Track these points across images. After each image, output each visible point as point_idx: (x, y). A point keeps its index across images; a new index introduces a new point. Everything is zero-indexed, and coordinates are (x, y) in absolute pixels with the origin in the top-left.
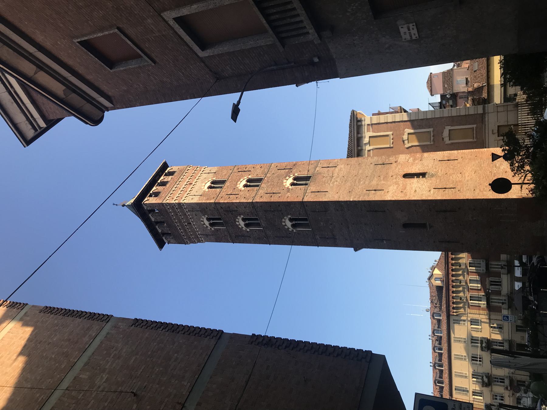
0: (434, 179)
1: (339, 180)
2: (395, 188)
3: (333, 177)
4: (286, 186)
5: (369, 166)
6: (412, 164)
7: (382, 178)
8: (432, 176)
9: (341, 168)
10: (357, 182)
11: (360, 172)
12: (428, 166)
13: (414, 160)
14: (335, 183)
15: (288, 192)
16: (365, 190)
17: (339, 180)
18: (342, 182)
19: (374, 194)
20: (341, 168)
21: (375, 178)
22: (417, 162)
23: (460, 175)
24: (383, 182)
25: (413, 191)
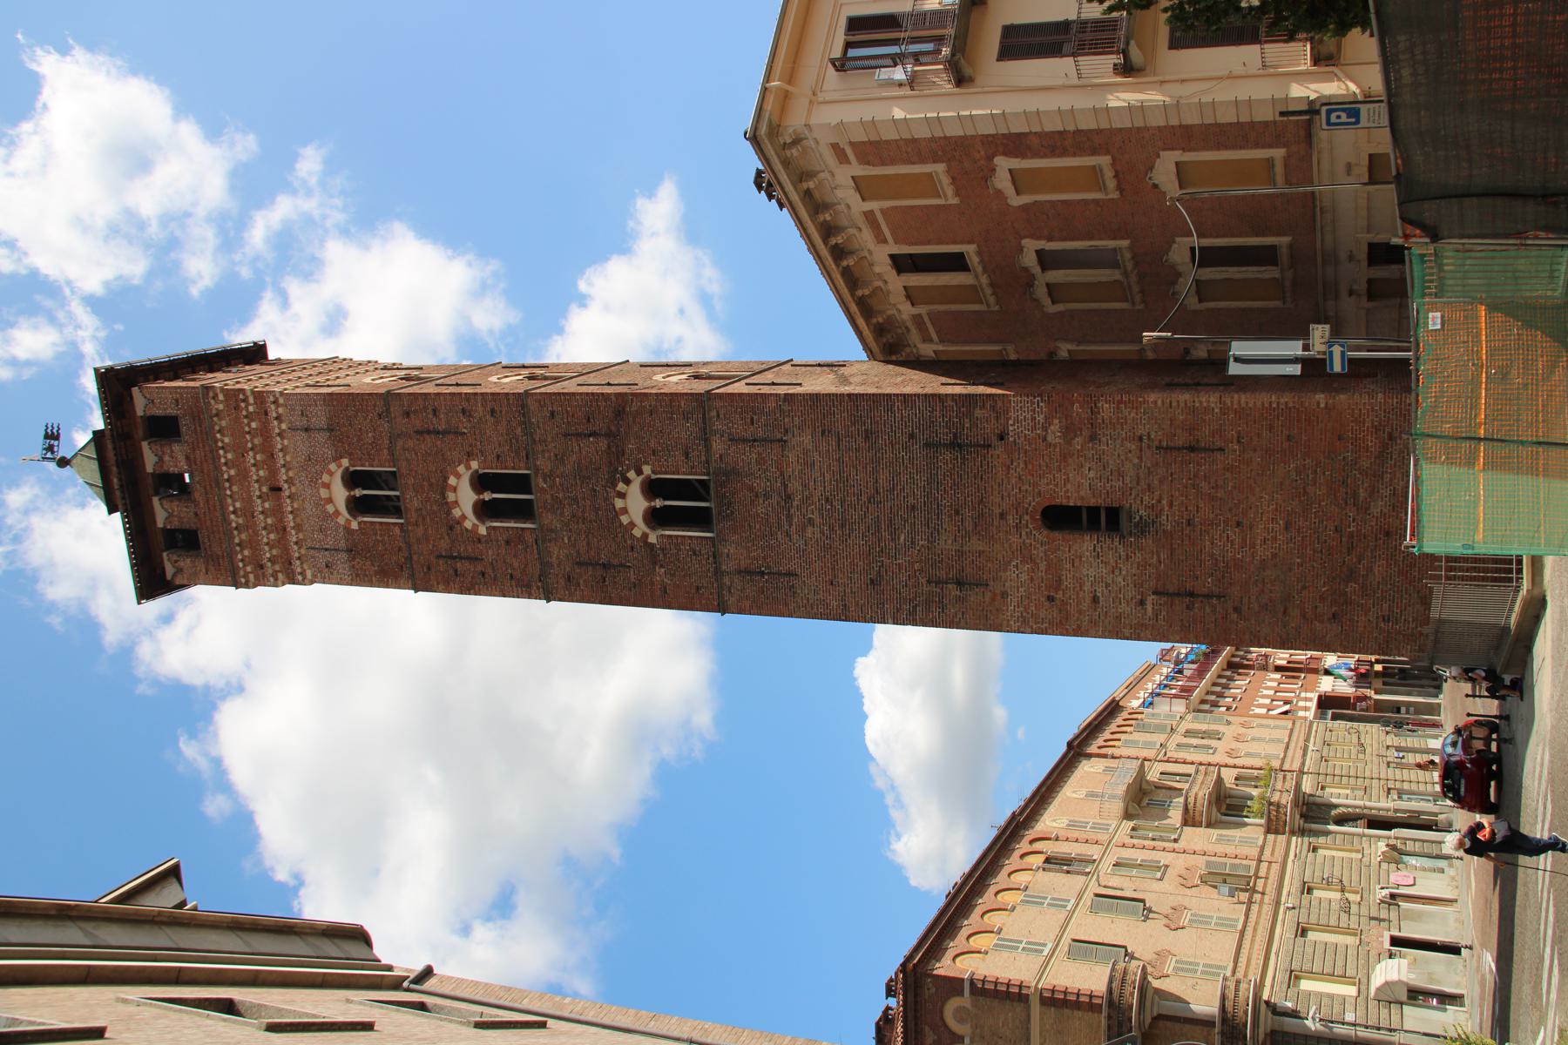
0: (1148, 542)
1: (816, 517)
2: (1024, 577)
3: (789, 498)
4: (637, 533)
5: (905, 448)
6: (1064, 457)
7: (969, 525)
8: (1142, 528)
9: (806, 453)
10: (885, 534)
11: (883, 477)
12: (1121, 475)
13: (1069, 431)
14: (810, 530)
15: (655, 562)
16: (924, 581)
17: (816, 517)
18: (832, 529)
19: (959, 599)
20: (806, 453)
21: (945, 518)
22: (1078, 443)
23: (1235, 535)
24: (976, 545)
25: (1088, 600)
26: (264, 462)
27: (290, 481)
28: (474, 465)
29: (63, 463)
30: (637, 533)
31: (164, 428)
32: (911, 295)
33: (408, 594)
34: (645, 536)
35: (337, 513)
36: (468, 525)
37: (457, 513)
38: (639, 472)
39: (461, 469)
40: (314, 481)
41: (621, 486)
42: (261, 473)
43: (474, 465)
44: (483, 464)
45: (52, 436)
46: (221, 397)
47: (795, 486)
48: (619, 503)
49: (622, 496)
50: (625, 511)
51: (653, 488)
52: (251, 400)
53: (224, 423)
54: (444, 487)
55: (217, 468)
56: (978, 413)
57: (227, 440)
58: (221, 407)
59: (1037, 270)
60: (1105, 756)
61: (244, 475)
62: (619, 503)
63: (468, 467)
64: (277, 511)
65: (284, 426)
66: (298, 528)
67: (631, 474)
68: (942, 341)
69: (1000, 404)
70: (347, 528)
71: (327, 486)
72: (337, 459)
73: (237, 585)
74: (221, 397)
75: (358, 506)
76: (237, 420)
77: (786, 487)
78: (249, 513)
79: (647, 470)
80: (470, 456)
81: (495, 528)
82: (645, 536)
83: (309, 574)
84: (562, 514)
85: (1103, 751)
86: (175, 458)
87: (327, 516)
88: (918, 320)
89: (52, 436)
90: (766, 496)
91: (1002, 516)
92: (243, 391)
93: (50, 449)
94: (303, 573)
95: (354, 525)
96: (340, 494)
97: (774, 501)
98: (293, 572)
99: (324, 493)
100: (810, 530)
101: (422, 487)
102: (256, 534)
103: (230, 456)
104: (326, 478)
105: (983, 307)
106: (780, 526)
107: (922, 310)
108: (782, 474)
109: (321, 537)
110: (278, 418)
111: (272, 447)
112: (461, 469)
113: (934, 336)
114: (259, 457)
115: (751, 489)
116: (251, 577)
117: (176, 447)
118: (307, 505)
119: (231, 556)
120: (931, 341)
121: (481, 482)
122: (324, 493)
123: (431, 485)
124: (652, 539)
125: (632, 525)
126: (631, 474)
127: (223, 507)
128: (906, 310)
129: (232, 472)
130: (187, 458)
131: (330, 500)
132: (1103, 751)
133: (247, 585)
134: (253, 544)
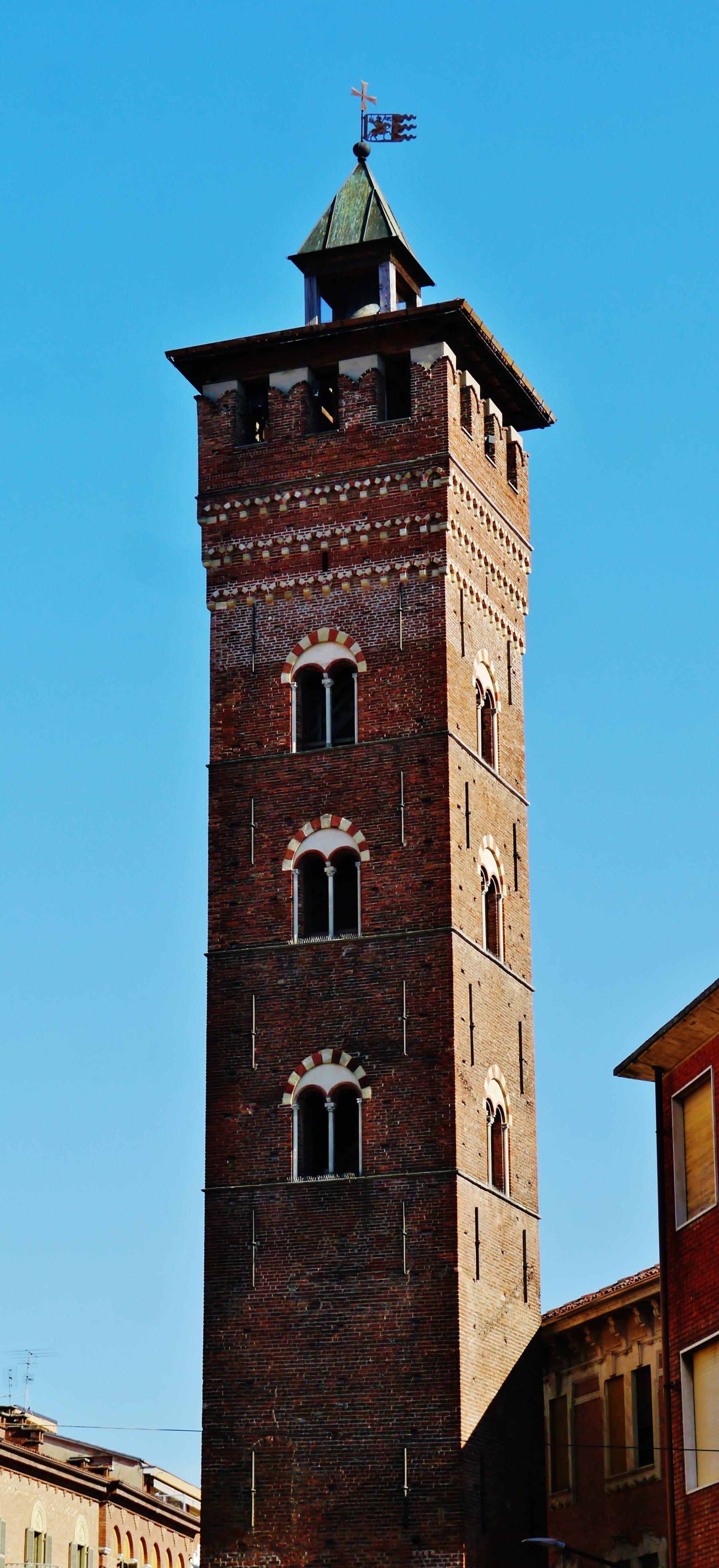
1: (320, 1310)
3: (341, 1277)
9: (393, 1298)
26: (359, 544)
27: (336, 583)
28: (365, 856)
29: (361, 152)
30: (294, 1079)
31: (397, 388)
32: (615, 1380)
33: (204, 756)
34: (289, 1089)
35: (299, 652)
36: (294, 845)
37: (307, 829)
38: (364, 1082)
39: (360, 837)
40: (337, 620)
41: (346, 1058)
42: (344, 542)
43: (365, 856)
44: (366, 867)
45: (397, 128)
46: (436, 483)
47: (355, 1284)
48: (327, 1054)
49: (336, 1060)
50: (318, 1062)
51: (345, 1094)
52: (434, 528)
53: (404, 487)
54: (338, 813)
55: (349, 477)
56: (442, 1512)
57: (383, 491)
58: (424, 484)
59: (641, 1552)
60: (102, 1541)
61: (341, 514)
62: (327, 1054)
63: (362, 846)
64: (297, 564)
65: (404, 577)
66: (279, 593)
67: (361, 1072)
68: (576, 1408)
69: (452, 1538)
70: (283, 667)
71: (332, 638)
72: (365, 654)
73: (202, 498)
74: (436, 483)
75: (309, 676)
76: (409, 508)
77: (353, 1273)
78: (295, 519)
79: (367, 1093)
80: (376, 850)
81: (290, 882)
82: (289, 1089)
83: (222, 606)
84: (311, 977)
85: (111, 1536)
86: (359, 413)
87: (295, 636)
88: (592, 1383)
89: (397, 128)
90: (341, 1248)
91: (330, 1543)
92: (445, 518)
93: (380, 129)
94: (222, 598)
95: (287, 678)
96: (324, 655)
97: (337, 1257)
98: (222, 584)
99: (323, 633)
100: (304, 1304)
101: (336, 780)
102: (269, 531)
103: (363, 494)
104: (342, 636)
105: (607, 1476)
106: (308, 1265)
107: (602, 1393)
108: (368, 1268)
109: (269, 627)
110: (413, 569)
111: (377, 560)
112: (360, 837)
113: (580, 1400)
114: (364, 538)
115: (350, 1229)
116: (213, 520)
117: (371, 411)
118: (307, 607)
119: (240, 492)
120: (576, 1395)
121: (345, 858)
122: (323, 633)
123: (339, 792)
124: (289, 1100)
125: (302, 1072)
126: (361, 1072)
127: (299, 484)
128: (603, 1372)
129: (343, 498)
130: (360, 427)
131: (315, 641)
132: (111, 1536)
133: (202, 514)
134: (255, 526)
